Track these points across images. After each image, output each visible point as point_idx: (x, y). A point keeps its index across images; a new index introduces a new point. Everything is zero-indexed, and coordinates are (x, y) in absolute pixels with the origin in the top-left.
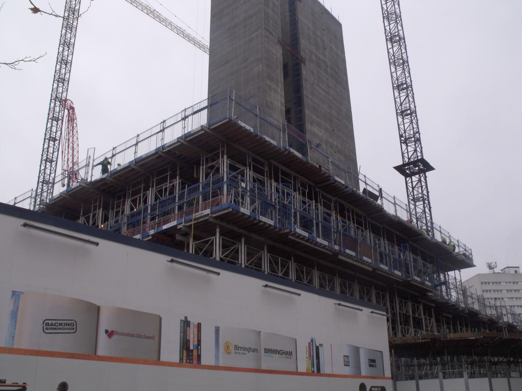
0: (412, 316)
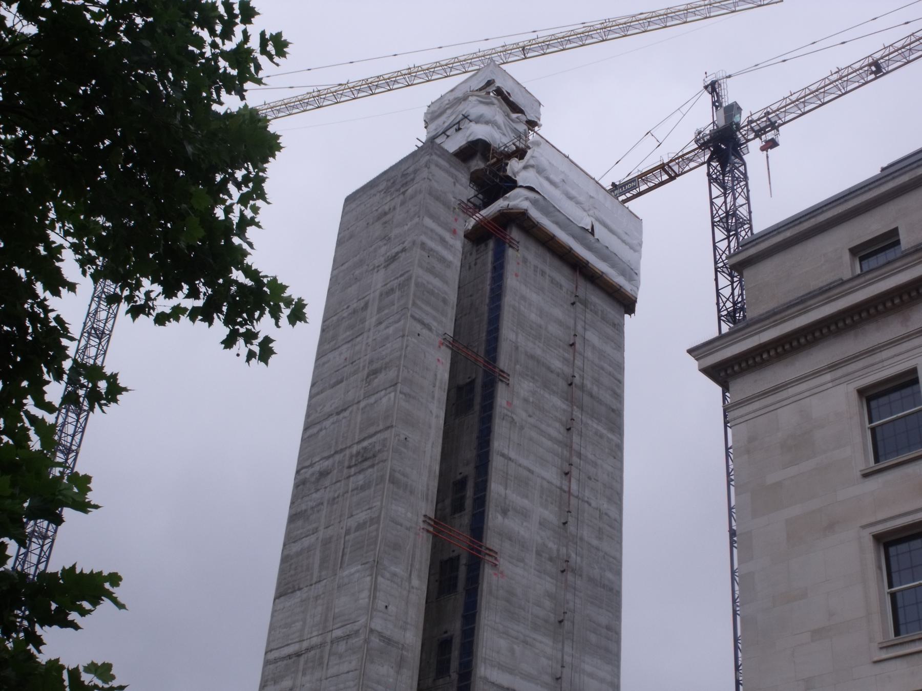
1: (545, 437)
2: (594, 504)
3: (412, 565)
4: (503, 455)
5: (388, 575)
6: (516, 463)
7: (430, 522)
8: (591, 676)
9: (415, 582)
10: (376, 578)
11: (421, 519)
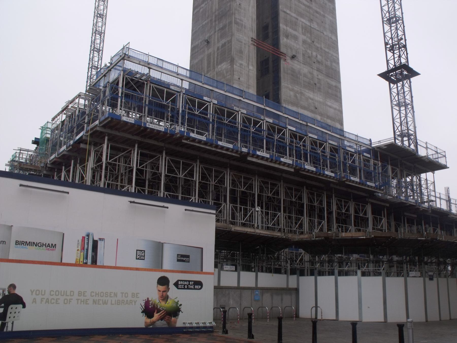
1: (301, 4)
2: (325, 33)
3: (249, 60)
5: (238, 65)
6: (290, 15)
7: (254, 41)
8: (330, 107)
9: (251, 67)
10: (233, 65)
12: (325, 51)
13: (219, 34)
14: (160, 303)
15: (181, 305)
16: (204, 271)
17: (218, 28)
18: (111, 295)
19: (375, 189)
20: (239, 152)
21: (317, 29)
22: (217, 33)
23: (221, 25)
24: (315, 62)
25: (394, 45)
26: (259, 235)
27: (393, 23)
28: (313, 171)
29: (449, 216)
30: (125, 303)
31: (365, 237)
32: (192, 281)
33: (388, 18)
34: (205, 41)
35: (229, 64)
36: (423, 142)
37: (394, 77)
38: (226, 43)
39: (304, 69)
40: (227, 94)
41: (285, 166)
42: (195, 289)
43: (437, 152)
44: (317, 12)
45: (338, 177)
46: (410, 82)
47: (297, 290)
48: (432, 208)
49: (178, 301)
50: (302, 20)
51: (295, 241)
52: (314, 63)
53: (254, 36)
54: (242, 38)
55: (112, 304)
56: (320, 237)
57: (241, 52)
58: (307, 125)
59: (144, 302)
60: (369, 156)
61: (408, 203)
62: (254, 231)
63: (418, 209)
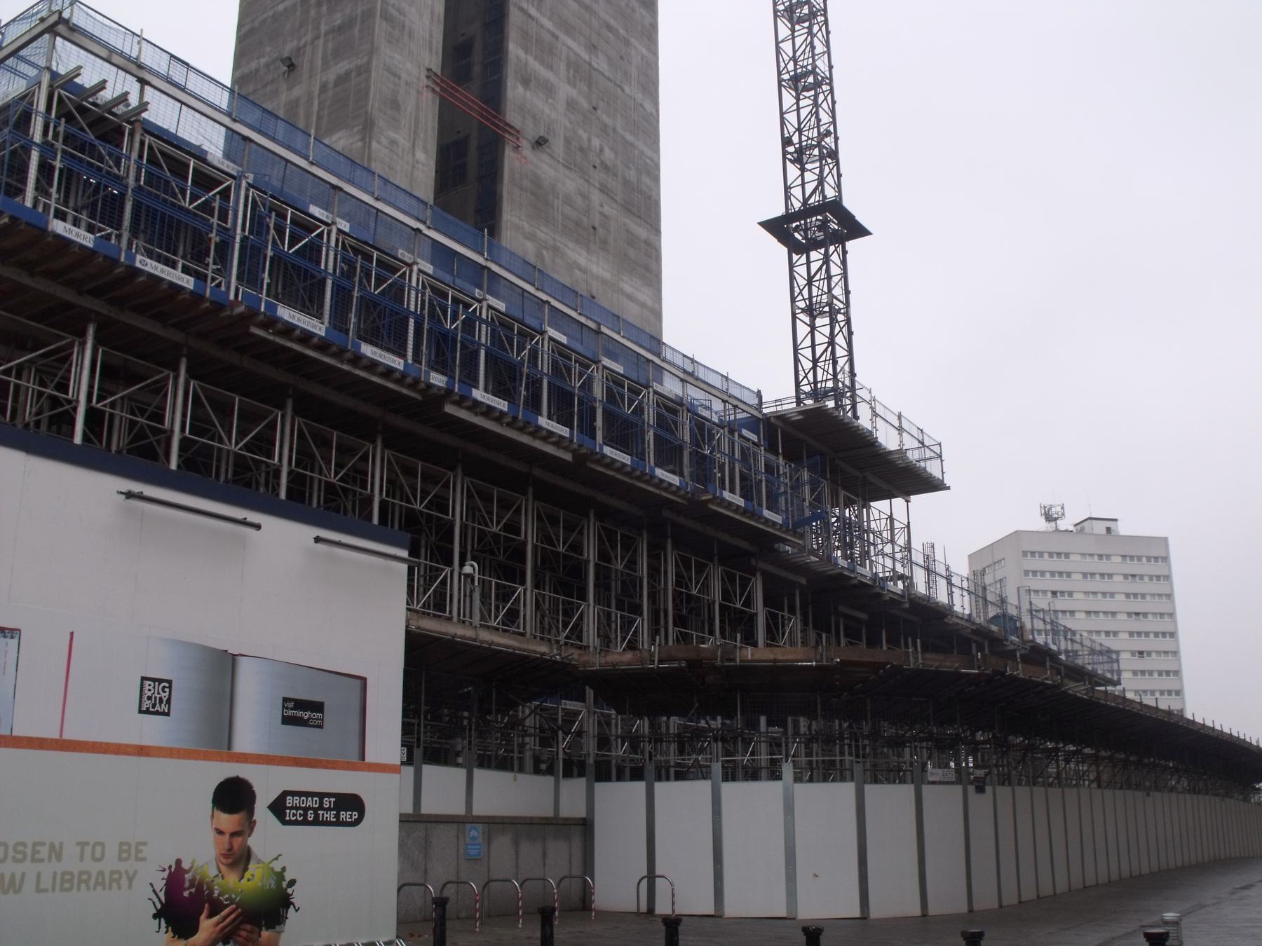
0: (721, 605)
3: (415, 133)
4: (522, 9)
5: (385, 141)
6: (537, 22)
7: (435, 79)
8: (630, 297)
9: (420, 155)
10: (370, 142)
11: (424, 73)
12: (623, 138)
13: (330, 45)
14: (223, 877)
15: (292, 883)
16: (369, 758)
17: (327, 27)
18: (38, 852)
19: (783, 532)
20: (422, 386)
21: (607, 74)
22: (321, 41)
23: (338, 19)
24: (597, 165)
25: (806, 149)
26: (489, 649)
27: (806, 89)
28: (624, 465)
29: (946, 620)
30: (92, 883)
31: (814, 663)
32: (329, 795)
33: (792, 73)
34: (283, 61)
35: (358, 137)
36: (893, 413)
37: (802, 233)
38: (351, 71)
39: (567, 180)
40: (379, 205)
41: (550, 443)
42: (339, 823)
43: (923, 443)
44: (609, 27)
45: (689, 490)
46: (845, 252)
47: (586, 826)
48: (912, 596)
49: (284, 869)
50: (570, 42)
51: (592, 671)
52: (595, 167)
53: (438, 70)
54: (401, 66)
55: (38, 890)
56: (676, 660)
57: (395, 105)
58: (598, 332)
59: (166, 874)
60: (754, 437)
61: (855, 578)
62: (474, 636)
63: (879, 595)
